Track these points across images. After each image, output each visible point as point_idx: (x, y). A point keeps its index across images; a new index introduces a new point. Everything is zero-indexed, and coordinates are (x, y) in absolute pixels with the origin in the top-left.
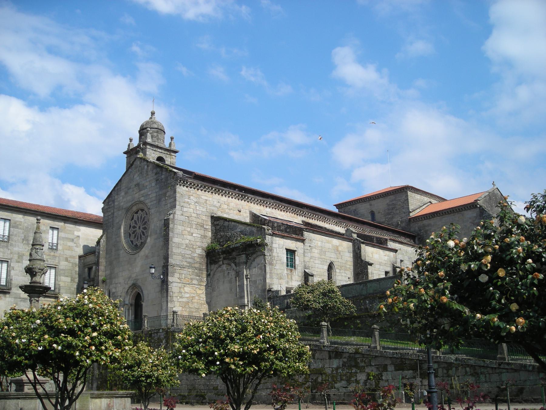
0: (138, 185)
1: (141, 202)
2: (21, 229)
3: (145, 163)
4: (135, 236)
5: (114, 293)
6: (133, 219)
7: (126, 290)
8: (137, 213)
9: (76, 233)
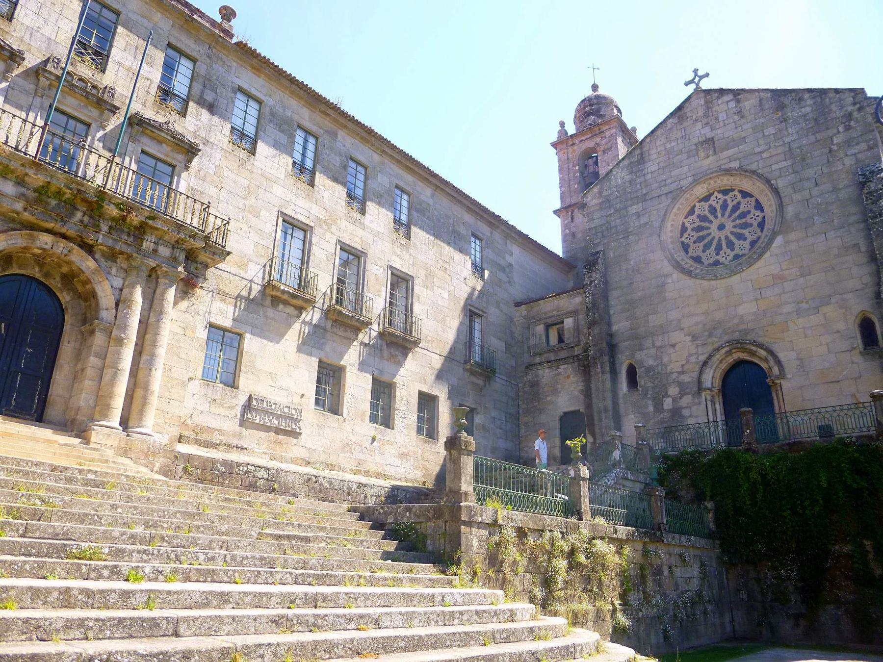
0: (710, 142)
1: (728, 172)
2: (428, 218)
5: (649, 369)
7: (702, 358)
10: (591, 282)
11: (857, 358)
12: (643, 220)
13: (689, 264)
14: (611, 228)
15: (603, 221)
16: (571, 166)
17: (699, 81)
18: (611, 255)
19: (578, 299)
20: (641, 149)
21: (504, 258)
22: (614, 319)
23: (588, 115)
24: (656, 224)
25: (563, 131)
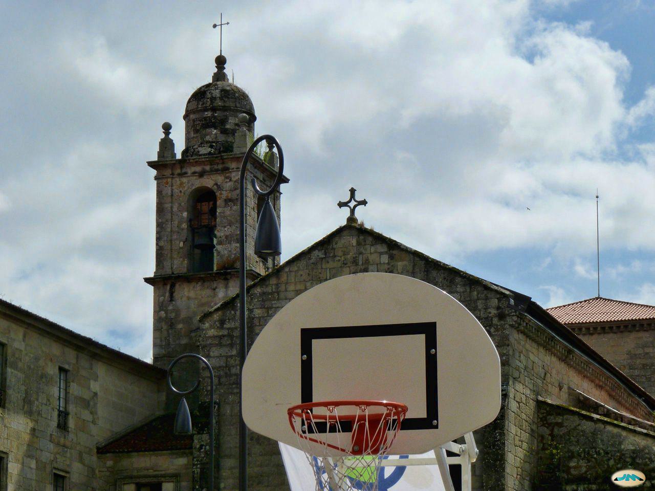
3: (382, 248)
9: (95, 386)
10: (201, 447)
14: (231, 375)
15: (222, 363)
16: (175, 209)
17: (355, 206)
19: (182, 461)
20: (278, 277)
21: (89, 388)
23: (208, 124)
25: (166, 145)
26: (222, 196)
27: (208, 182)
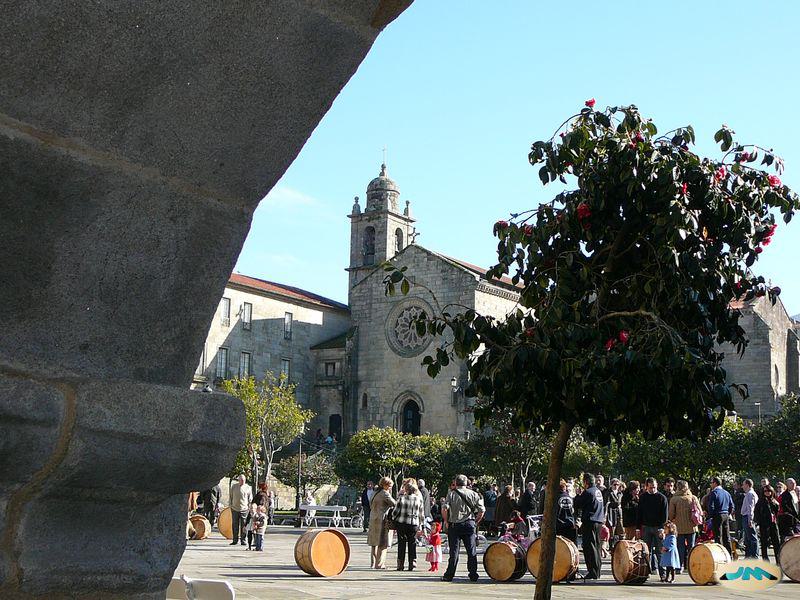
4: (406, 336)
6: (401, 315)
8: (409, 309)
11: (450, 408)
12: (378, 314)
13: (396, 345)
18: (361, 329)
22: (359, 368)
24: (384, 319)
25: (356, 207)
26: (377, 230)
27: (371, 224)
